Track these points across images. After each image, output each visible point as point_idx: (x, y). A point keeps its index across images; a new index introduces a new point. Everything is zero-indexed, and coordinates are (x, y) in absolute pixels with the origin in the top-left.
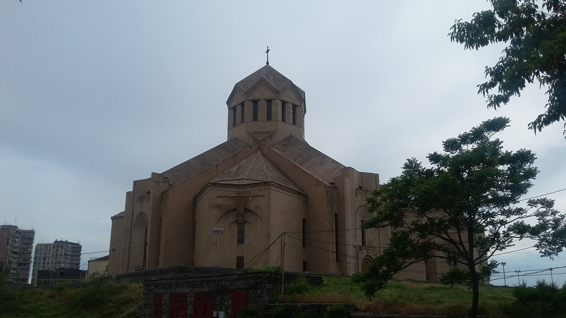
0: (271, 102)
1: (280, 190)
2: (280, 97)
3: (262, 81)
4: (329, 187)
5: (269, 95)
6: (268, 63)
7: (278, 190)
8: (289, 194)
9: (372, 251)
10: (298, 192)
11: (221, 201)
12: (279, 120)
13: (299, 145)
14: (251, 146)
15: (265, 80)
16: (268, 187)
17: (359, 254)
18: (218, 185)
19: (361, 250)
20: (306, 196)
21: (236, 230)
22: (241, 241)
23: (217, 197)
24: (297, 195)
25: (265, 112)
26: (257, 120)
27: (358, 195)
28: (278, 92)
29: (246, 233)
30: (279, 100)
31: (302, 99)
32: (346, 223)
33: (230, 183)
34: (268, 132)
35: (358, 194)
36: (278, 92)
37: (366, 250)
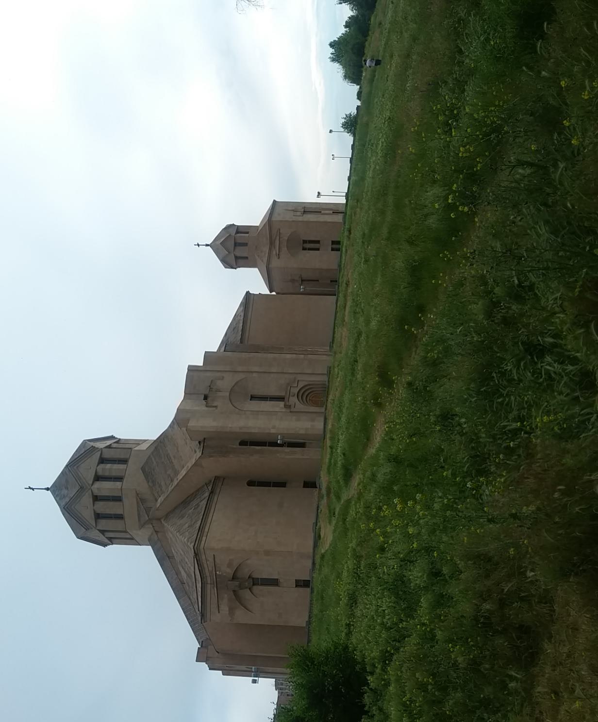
1: (206, 530)
4: (202, 454)
5: (87, 499)
6: (47, 489)
7: (205, 534)
8: (212, 511)
10: (210, 493)
11: (225, 608)
12: (120, 487)
13: (153, 463)
14: (156, 531)
15: (66, 504)
16: (202, 550)
17: (295, 410)
19: (290, 406)
20: (217, 478)
22: (275, 582)
24: (214, 496)
25: (111, 504)
26: (122, 515)
27: (215, 404)
28: (81, 488)
29: (265, 576)
32: (253, 431)
33: (200, 594)
34: (138, 503)
36: (81, 487)
37: (291, 398)
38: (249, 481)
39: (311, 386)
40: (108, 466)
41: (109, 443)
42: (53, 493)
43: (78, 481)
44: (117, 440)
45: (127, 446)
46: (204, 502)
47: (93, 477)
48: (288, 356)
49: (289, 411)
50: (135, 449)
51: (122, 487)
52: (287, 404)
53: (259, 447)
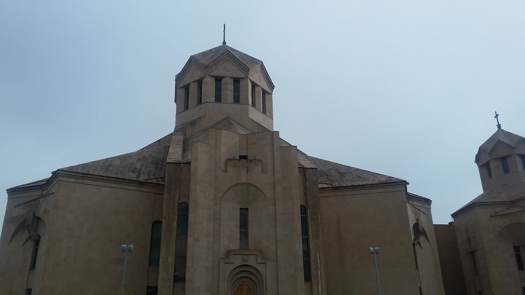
3: (192, 60)
5: (198, 74)
6: (224, 43)
7: (81, 181)
8: (114, 185)
9: (255, 256)
12: (207, 101)
18: (17, 190)
21: (31, 249)
23: (15, 207)
24: (136, 186)
27: (230, 169)
28: (206, 67)
30: (208, 77)
35: (227, 166)
36: (206, 66)
37: (240, 257)
40: (231, 87)
41: (264, 85)
42: (218, 49)
43: (212, 63)
44: (270, 92)
46: (133, 176)
48: (299, 247)
49: (220, 257)
50: (251, 108)
51: (208, 102)
53: (175, 226)
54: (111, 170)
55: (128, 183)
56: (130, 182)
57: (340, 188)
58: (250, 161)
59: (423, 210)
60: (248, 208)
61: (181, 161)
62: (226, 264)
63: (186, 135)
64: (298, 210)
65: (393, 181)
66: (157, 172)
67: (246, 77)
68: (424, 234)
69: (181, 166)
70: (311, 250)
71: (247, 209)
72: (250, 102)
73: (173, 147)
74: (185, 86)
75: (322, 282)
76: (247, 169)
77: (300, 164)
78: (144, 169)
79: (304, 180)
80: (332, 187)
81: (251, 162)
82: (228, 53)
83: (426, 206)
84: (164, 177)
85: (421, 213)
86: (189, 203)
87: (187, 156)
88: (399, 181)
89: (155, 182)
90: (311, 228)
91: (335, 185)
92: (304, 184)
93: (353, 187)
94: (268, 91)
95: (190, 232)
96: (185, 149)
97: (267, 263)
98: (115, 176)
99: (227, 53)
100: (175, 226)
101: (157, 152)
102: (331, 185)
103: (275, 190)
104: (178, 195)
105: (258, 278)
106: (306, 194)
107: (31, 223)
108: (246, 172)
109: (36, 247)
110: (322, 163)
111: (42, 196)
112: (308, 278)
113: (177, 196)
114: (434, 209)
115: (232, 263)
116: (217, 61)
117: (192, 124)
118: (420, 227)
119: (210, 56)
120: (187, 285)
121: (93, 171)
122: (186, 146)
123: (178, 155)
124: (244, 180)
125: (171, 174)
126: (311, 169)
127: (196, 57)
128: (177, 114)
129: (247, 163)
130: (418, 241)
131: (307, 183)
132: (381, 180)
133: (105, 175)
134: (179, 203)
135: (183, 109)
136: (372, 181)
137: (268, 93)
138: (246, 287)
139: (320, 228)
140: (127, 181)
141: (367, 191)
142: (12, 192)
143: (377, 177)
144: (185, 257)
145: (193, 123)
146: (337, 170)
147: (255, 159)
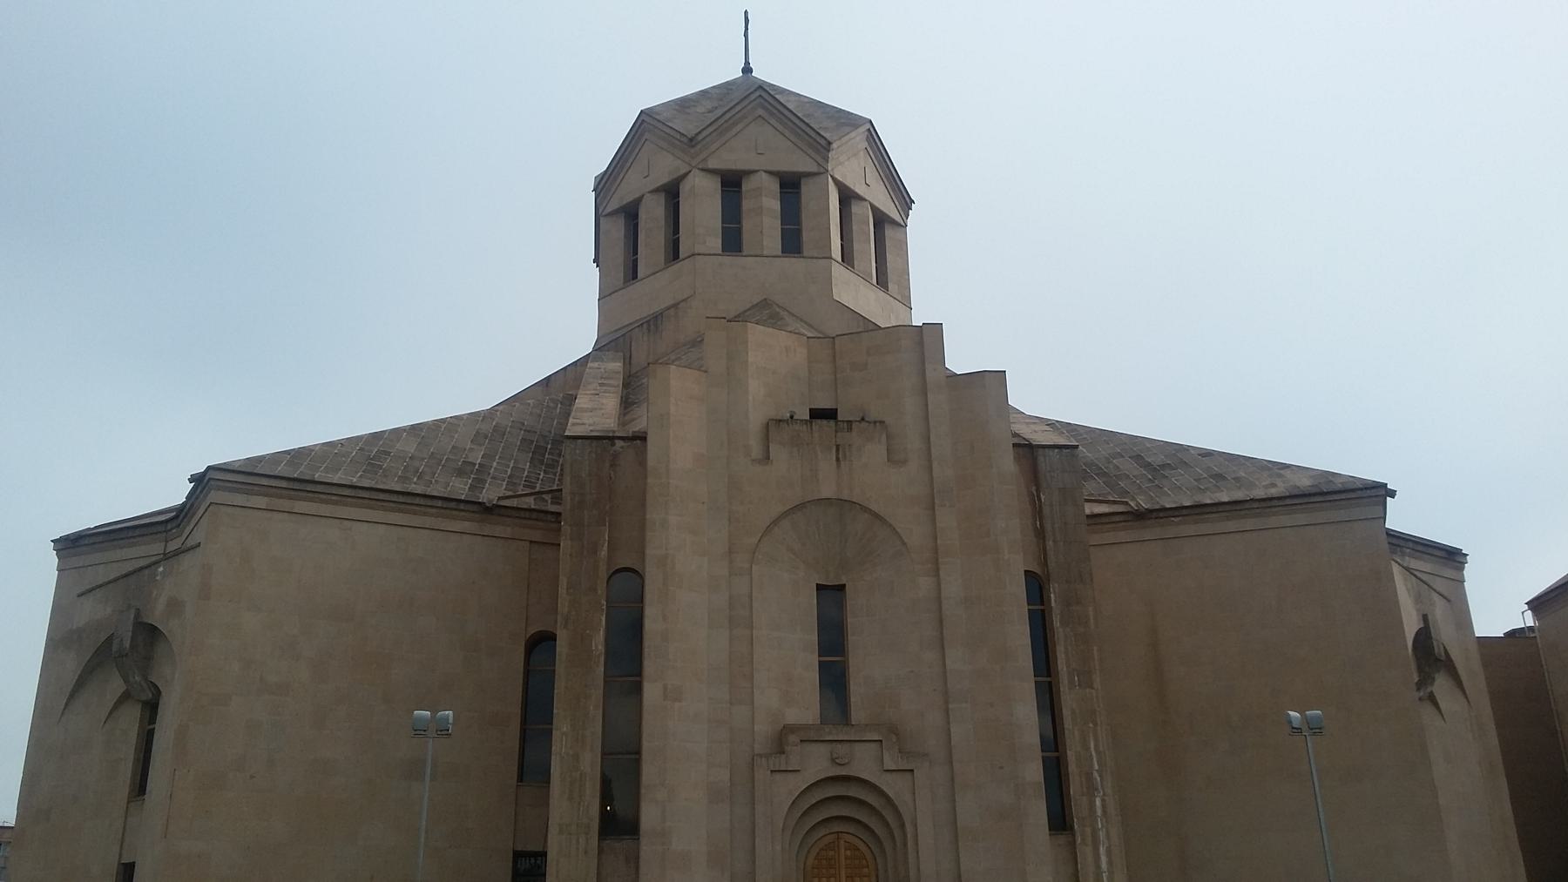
0: (677, 195)
2: (705, 160)
5: (664, 166)
6: (747, 70)
9: (873, 745)
23: (79, 596)
28: (692, 141)
30: (695, 172)
31: (823, 142)
35: (771, 444)
36: (691, 140)
37: (823, 749)
38: (540, 631)
39: (897, 833)
40: (773, 204)
42: (727, 88)
43: (711, 129)
44: (896, 217)
45: (866, 249)
46: (460, 488)
47: (734, 168)
48: (1026, 712)
50: (838, 271)
51: (699, 254)
52: (793, 738)
53: (601, 648)
54: (385, 470)
55: (442, 508)
56: (450, 505)
57: (1155, 514)
58: (845, 424)
59: (1439, 584)
60: (845, 585)
61: (614, 432)
62: (778, 776)
63: (632, 362)
64: (1019, 589)
65: (1340, 485)
66: (539, 474)
67: (822, 170)
68: (1449, 666)
69: (614, 448)
70: (1068, 723)
71: (842, 588)
72: (836, 252)
73: (588, 392)
74: (625, 206)
75: (1108, 836)
76: (838, 450)
77: (1016, 435)
78: (495, 464)
79: (1034, 488)
80: (1127, 513)
81: (850, 429)
82: (760, 96)
83: (1449, 573)
84: (561, 490)
85: (1436, 597)
86: (644, 568)
87: (633, 420)
88: (1361, 486)
89: (533, 507)
90: (1063, 649)
91: (1138, 504)
92: (1033, 502)
93: (1199, 510)
94: (895, 218)
95: (649, 667)
96: (630, 400)
97: (915, 771)
98: (398, 488)
99: (757, 94)
100: (600, 647)
101: (540, 416)
102: (1122, 506)
103: (933, 521)
104: (606, 544)
105: (887, 825)
106: (1040, 534)
107: (128, 646)
108: (835, 463)
109: (149, 724)
110: (1085, 436)
111: (167, 557)
112: (1060, 821)
113: (605, 548)
114: (1475, 580)
115: (798, 771)
116: (726, 121)
117: (649, 325)
118: (1435, 643)
119: (703, 110)
120: (647, 848)
121: (327, 470)
122: (631, 392)
123: (603, 414)
124: (827, 491)
125: (584, 475)
126: (1056, 450)
127: (658, 114)
128: (603, 297)
129: (836, 432)
130: (1429, 690)
131: (1043, 497)
132: (1298, 484)
133: (366, 483)
134: (611, 572)
135: (622, 281)
136: (1266, 487)
137: (894, 223)
138: (848, 853)
139: (1095, 648)
140: (439, 503)
141: (1249, 524)
142: (70, 546)
143: (1280, 476)
144: (638, 752)
145: (653, 323)
146: (1138, 458)
147: (863, 419)
